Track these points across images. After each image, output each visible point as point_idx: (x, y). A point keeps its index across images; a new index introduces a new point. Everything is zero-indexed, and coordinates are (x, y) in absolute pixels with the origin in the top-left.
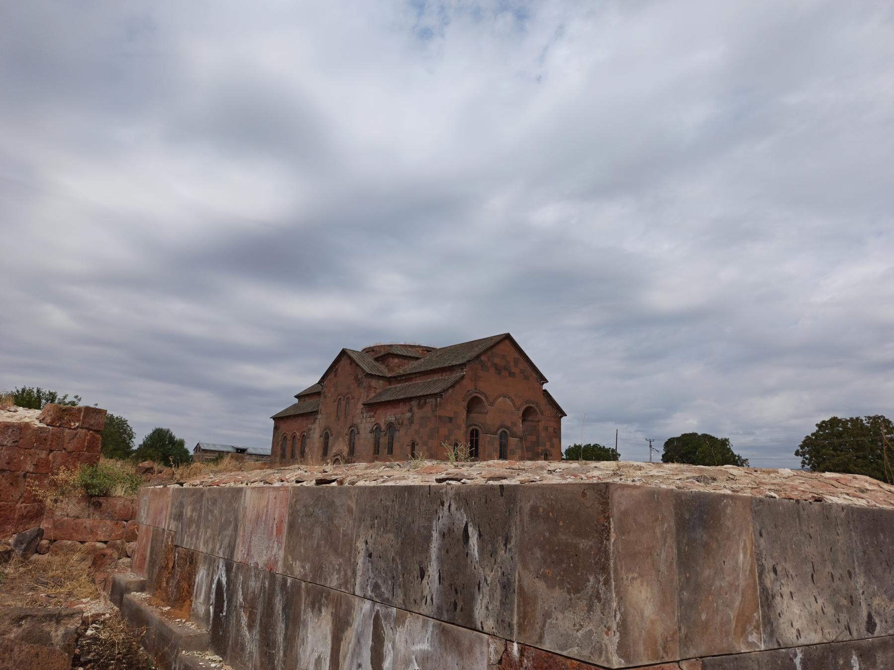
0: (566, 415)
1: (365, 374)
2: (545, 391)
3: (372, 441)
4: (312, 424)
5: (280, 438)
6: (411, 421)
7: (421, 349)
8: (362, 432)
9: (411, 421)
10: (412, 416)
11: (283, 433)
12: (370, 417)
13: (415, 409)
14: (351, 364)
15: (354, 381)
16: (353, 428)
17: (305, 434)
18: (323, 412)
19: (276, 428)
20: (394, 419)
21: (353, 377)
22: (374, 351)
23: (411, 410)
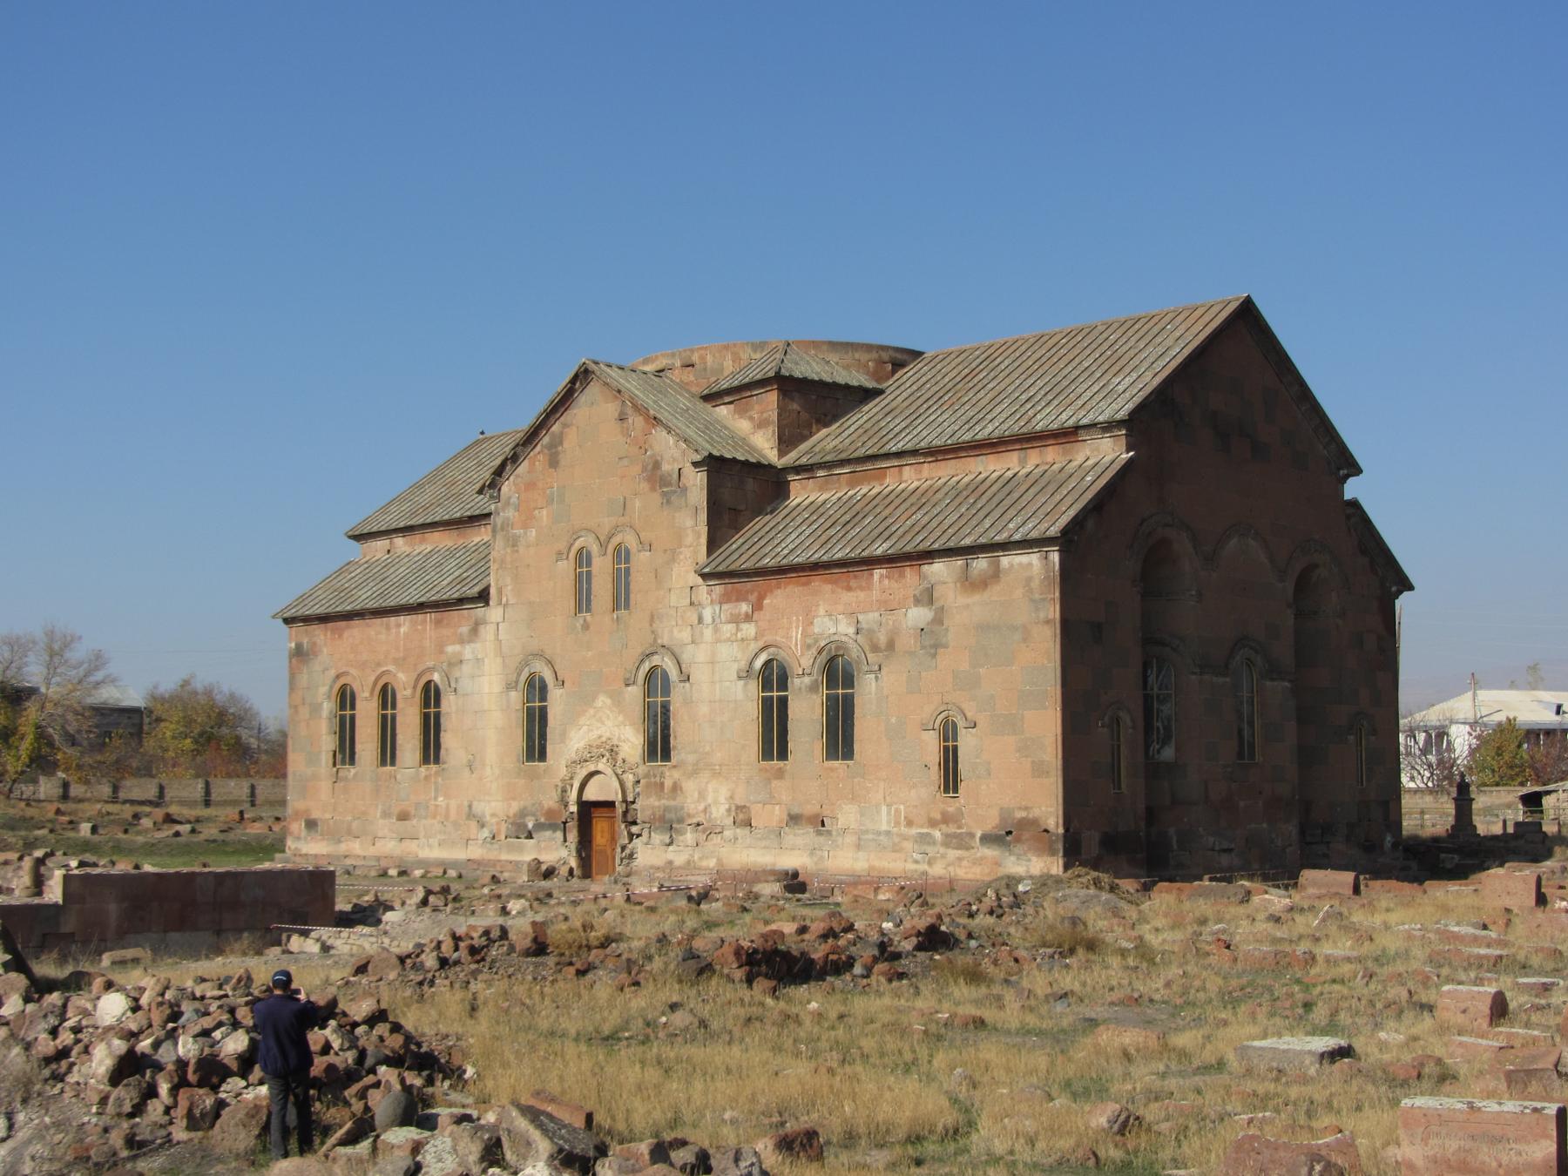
0: (1411, 588)
2: (1355, 504)
3: (753, 710)
4: (462, 642)
5: (323, 690)
6: (932, 639)
7: (874, 355)
8: (699, 674)
9: (932, 639)
10: (938, 620)
11: (332, 673)
12: (736, 620)
13: (951, 596)
15: (644, 486)
16: (656, 660)
17: (436, 677)
18: (509, 595)
19: (300, 654)
20: (851, 630)
21: (637, 469)
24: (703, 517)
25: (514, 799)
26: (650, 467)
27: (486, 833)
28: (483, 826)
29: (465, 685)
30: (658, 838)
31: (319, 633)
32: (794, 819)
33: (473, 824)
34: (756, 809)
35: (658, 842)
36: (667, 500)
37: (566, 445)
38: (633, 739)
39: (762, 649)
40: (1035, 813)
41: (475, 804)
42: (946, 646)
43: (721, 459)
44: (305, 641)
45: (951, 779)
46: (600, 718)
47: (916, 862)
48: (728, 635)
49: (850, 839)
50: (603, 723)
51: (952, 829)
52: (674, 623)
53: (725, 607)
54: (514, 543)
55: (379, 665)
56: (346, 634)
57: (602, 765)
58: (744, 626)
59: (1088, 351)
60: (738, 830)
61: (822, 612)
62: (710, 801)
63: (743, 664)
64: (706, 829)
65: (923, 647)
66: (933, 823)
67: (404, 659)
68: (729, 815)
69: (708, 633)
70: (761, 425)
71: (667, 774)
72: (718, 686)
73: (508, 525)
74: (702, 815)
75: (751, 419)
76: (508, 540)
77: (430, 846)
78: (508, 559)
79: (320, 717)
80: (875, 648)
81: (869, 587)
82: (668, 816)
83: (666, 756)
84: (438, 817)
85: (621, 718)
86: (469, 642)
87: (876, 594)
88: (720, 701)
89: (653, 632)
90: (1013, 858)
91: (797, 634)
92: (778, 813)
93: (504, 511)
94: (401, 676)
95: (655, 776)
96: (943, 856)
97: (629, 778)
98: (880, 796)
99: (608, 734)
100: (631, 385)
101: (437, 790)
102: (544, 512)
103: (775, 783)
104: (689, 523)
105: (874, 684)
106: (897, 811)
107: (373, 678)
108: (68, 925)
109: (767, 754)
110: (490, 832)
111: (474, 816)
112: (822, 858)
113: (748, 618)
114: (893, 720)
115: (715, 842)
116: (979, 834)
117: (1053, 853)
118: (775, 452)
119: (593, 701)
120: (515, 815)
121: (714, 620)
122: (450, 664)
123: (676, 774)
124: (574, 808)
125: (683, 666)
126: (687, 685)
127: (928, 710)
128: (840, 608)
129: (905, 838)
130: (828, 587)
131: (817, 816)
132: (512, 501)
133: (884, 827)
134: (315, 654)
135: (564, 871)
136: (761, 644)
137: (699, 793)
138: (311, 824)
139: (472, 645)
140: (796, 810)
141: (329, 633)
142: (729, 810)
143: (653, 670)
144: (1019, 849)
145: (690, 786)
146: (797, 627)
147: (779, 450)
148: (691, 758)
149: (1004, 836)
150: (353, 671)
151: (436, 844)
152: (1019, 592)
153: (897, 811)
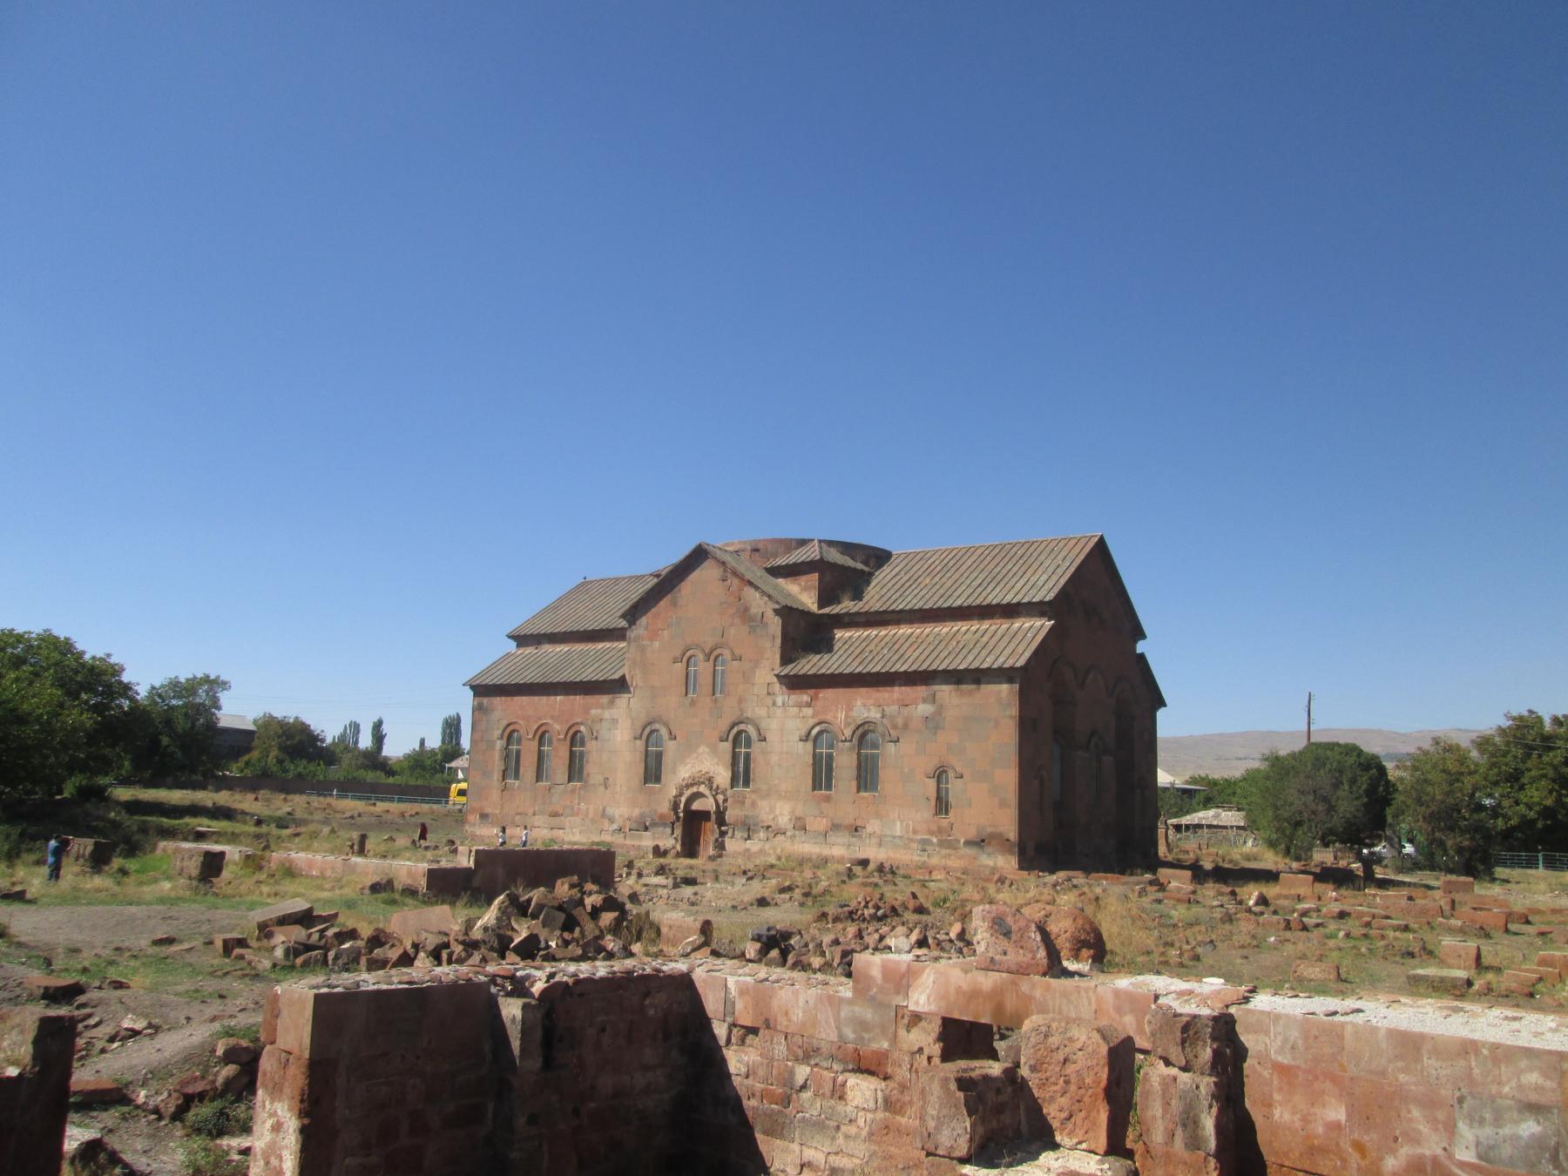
0: (1164, 705)
1: (777, 607)
2: (1142, 657)
4: (603, 708)
9: (933, 723)
10: (939, 712)
11: (505, 722)
12: (800, 705)
15: (737, 621)
16: (742, 727)
17: (582, 728)
19: (478, 710)
20: (879, 716)
22: (757, 550)
24: (778, 641)
27: (615, 826)
28: (613, 822)
29: (604, 733)
30: (738, 834)
31: (497, 701)
32: (835, 827)
33: (606, 822)
36: (753, 630)
40: (1001, 829)
42: (943, 728)
43: (791, 609)
45: (942, 805)
47: (920, 856)
49: (874, 841)
51: (944, 837)
52: (755, 704)
54: (643, 650)
55: (540, 719)
57: (702, 789)
59: (1006, 559)
60: (797, 832)
61: (859, 703)
62: (777, 812)
63: (804, 732)
64: (775, 831)
66: (931, 833)
69: (779, 712)
70: (805, 589)
72: (785, 744)
75: (800, 585)
77: (573, 834)
80: (895, 727)
83: (747, 783)
85: (715, 761)
89: (741, 709)
90: (985, 856)
91: (841, 715)
92: (821, 824)
96: (939, 852)
97: (720, 798)
98: (896, 814)
99: (706, 770)
100: (728, 559)
101: (579, 799)
103: (824, 805)
104: (768, 645)
105: (893, 749)
106: (908, 825)
108: (476, 882)
109: (816, 785)
112: (855, 851)
113: (809, 705)
114: (906, 770)
116: (962, 841)
117: (1012, 853)
118: (816, 605)
119: (697, 748)
121: (783, 704)
122: (593, 721)
123: (754, 796)
124: (681, 815)
125: (762, 732)
126: (764, 743)
127: (931, 765)
128: (872, 702)
129: (912, 840)
131: (852, 826)
133: (898, 834)
134: (493, 711)
135: (673, 852)
136: (816, 720)
138: (484, 816)
140: (837, 821)
142: (790, 820)
143: (739, 733)
144: (989, 850)
147: (819, 604)
148: (764, 788)
149: (980, 843)
150: (521, 722)
153: (908, 825)
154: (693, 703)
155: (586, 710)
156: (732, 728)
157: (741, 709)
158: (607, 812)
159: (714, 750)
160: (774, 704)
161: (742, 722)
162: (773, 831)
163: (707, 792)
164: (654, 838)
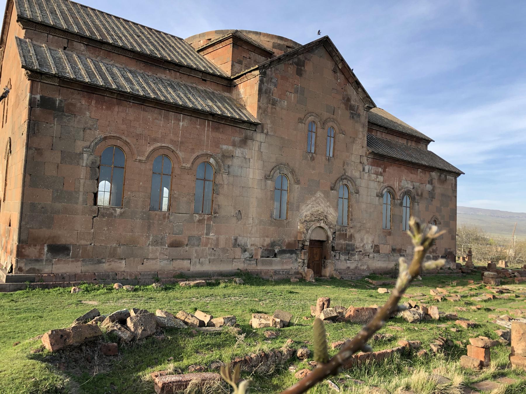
4: (234, 145)
8: (362, 191)
10: (433, 190)
11: (99, 134)
12: (377, 174)
14: (335, 72)
15: (343, 106)
16: (345, 182)
17: (212, 160)
20: (412, 187)
21: (340, 97)
23: (431, 182)
25: (267, 237)
26: (346, 99)
27: (247, 255)
28: (245, 251)
33: (238, 250)
34: (381, 246)
35: (343, 259)
37: (306, 68)
38: (333, 214)
39: (385, 188)
41: (240, 238)
44: (58, 99)
46: (318, 202)
48: (373, 179)
50: (319, 204)
51: (435, 255)
53: (373, 167)
54: (274, 103)
55: (155, 140)
56: (116, 109)
57: (322, 225)
58: (379, 177)
60: (375, 254)
65: (429, 197)
67: (182, 143)
68: (372, 249)
71: (348, 230)
72: (369, 197)
73: (270, 92)
74: (362, 248)
76: (270, 101)
77: (202, 264)
78: (269, 110)
79: (78, 164)
80: (418, 195)
81: (417, 175)
82: (349, 248)
84: (209, 246)
85: (328, 204)
86: (240, 147)
87: (419, 177)
88: (370, 203)
89: (344, 169)
93: (268, 84)
94: (181, 154)
95: (343, 231)
99: (322, 210)
102: (293, 95)
103: (388, 237)
104: (361, 129)
107: (150, 149)
110: (250, 255)
111: (239, 245)
113: (381, 174)
115: (366, 259)
119: (315, 194)
120: (267, 245)
122: (223, 156)
123: (352, 231)
126: (357, 195)
130: (406, 171)
132: (273, 80)
136: (386, 184)
137: (361, 239)
139: (242, 149)
140: (394, 247)
141: (93, 102)
142: (372, 247)
145: (357, 236)
146: (397, 182)
148: (359, 225)
151: (207, 262)
152: (450, 187)
154: (313, 159)
155: (217, 144)
156: (340, 181)
157: (344, 169)
158: (239, 242)
159: (327, 195)
160: (364, 170)
161: (346, 179)
162: (363, 254)
163: (326, 227)
164: (283, 263)
